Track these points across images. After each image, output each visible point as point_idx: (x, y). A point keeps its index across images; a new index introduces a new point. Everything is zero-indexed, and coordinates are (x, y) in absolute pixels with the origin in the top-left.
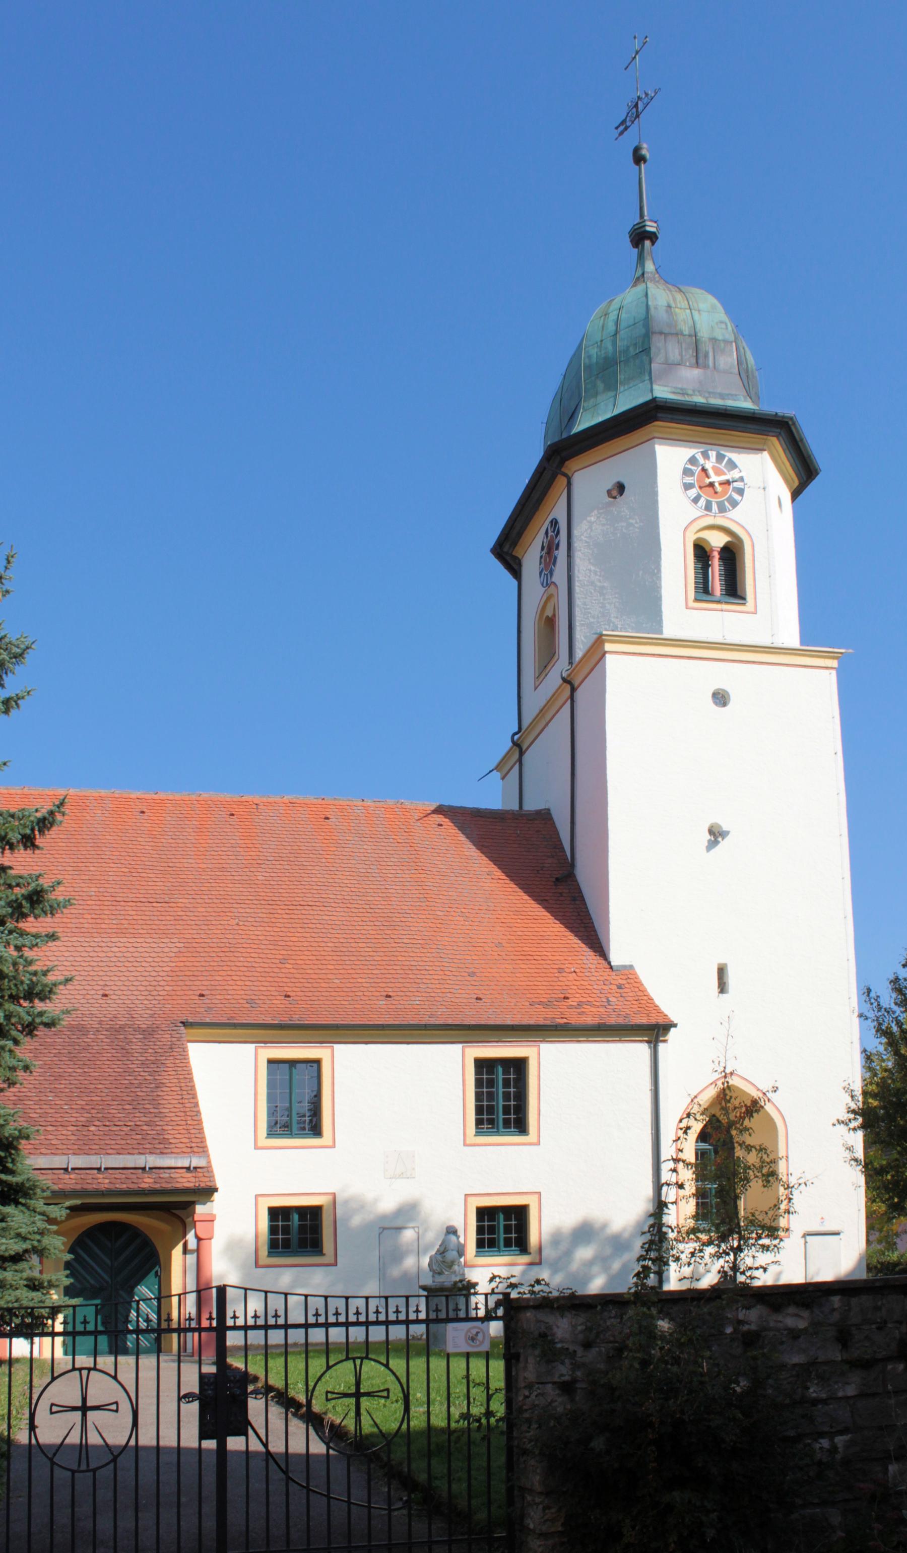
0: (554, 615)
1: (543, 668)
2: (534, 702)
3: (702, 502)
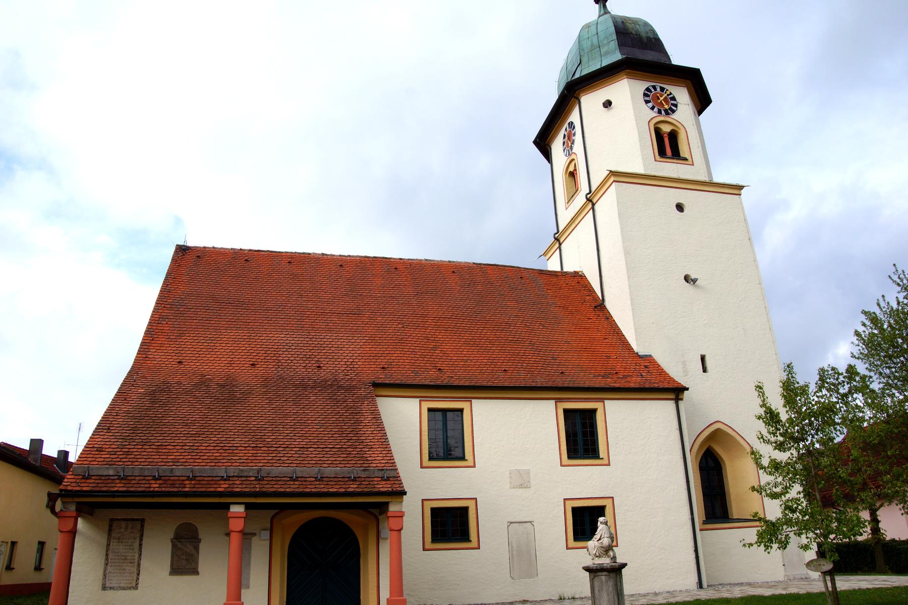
0: (575, 170)
1: (571, 198)
2: (565, 217)
3: (656, 109)
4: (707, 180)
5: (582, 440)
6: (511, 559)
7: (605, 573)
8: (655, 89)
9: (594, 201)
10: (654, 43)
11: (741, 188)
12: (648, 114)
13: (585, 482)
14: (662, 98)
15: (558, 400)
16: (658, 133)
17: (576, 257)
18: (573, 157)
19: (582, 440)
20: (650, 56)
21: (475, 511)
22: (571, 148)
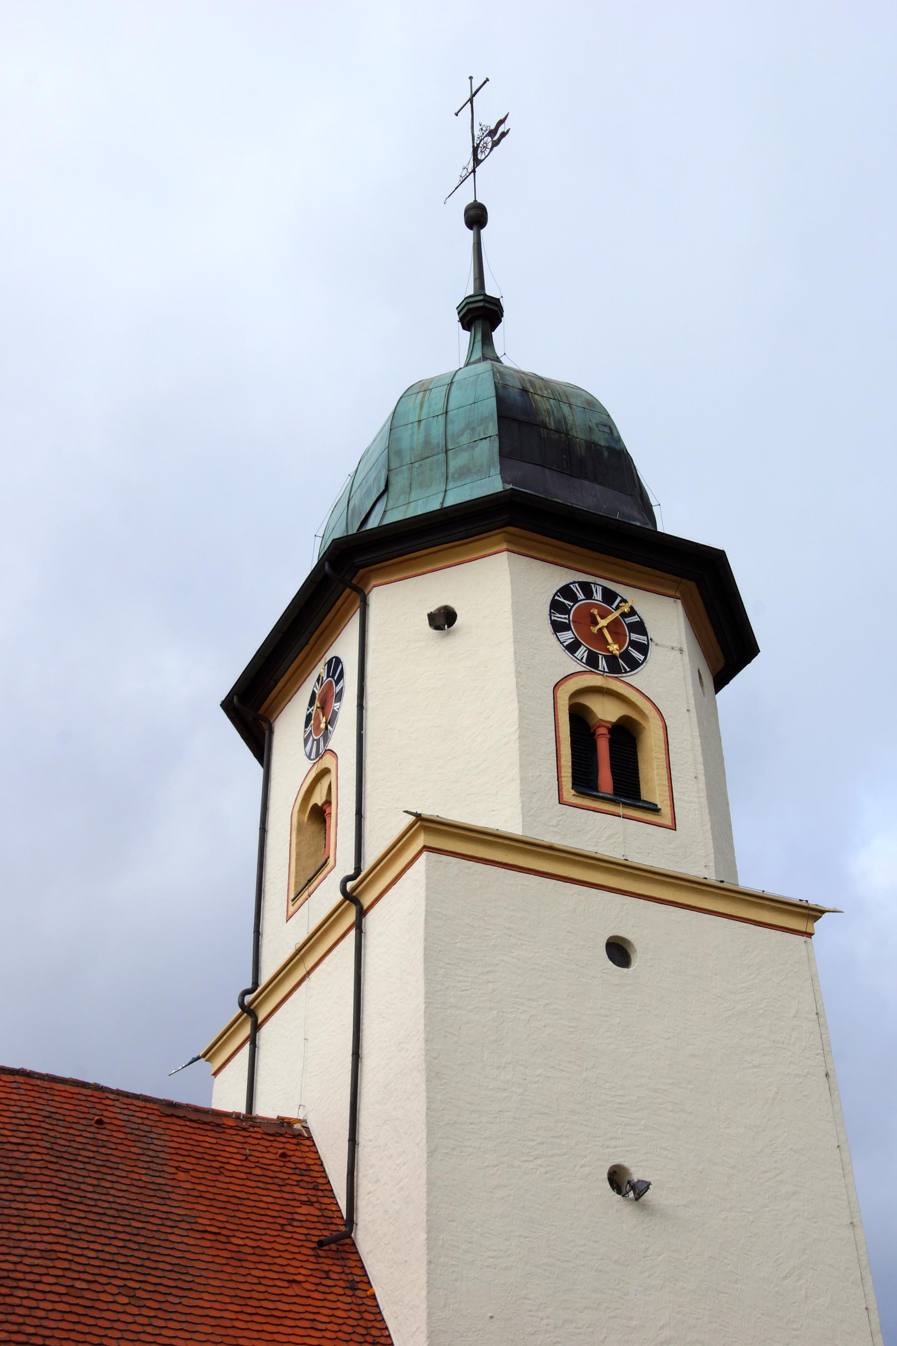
0: (328, 802)
1: (304, 886)
2: (282, 940)
3: (582, 652)
4: (712, 877)
8: (588, 593)
9: (366, 902)
10: (612, 463)
11: (814, 913)
12: (558, 662)
14: (603, 623)
16: (581, 722)
17: (293, 1075)
18: (327, 762)
20: (588, 497)
22: (326, 737)
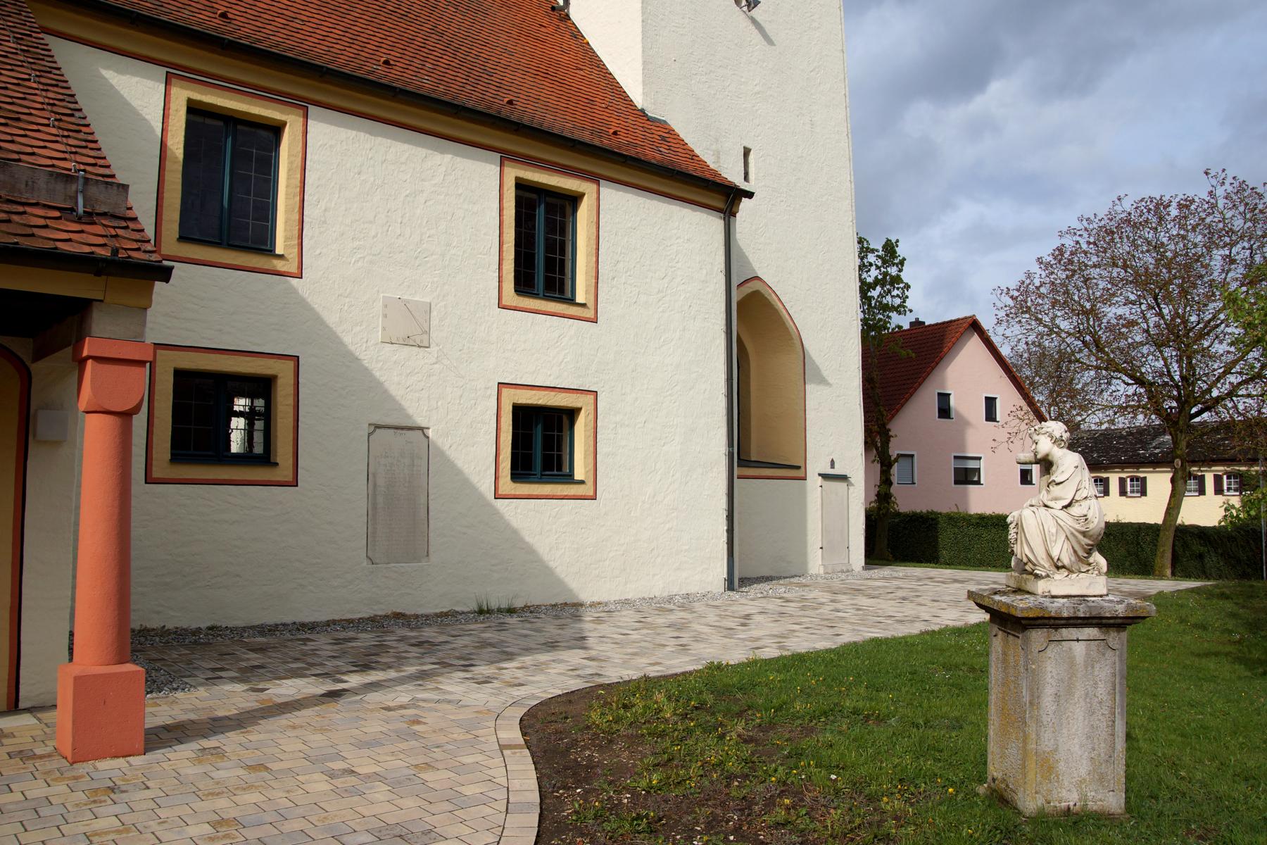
5: (542, 261)
6: (372, 513)
7: (1092, 632)
13: (541, 351)
15: (507, 157)
19: (542, 261)
21: (291, 390)
